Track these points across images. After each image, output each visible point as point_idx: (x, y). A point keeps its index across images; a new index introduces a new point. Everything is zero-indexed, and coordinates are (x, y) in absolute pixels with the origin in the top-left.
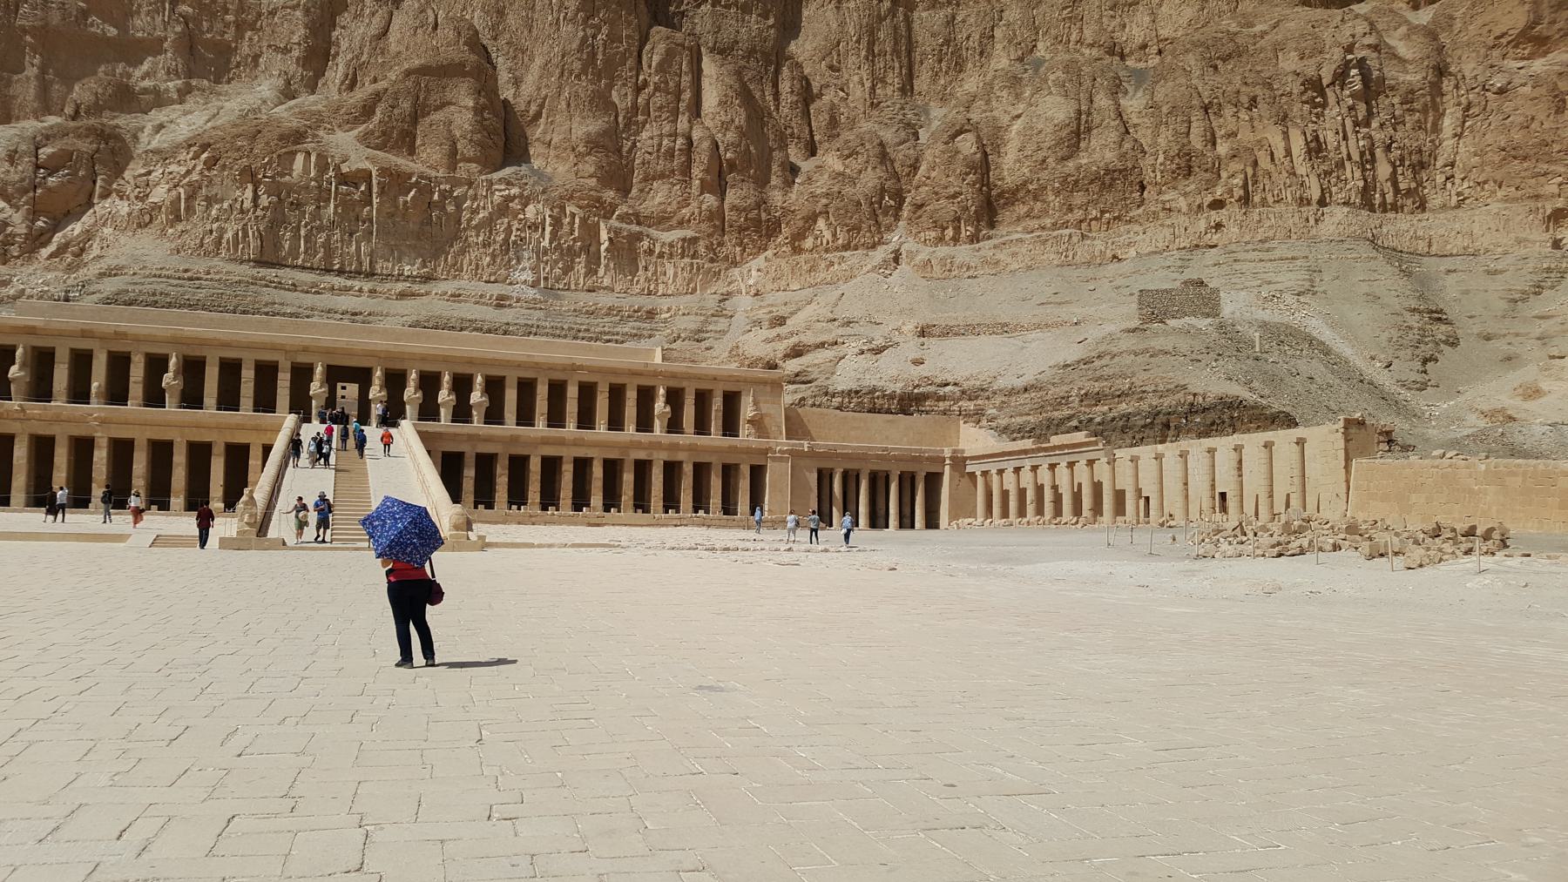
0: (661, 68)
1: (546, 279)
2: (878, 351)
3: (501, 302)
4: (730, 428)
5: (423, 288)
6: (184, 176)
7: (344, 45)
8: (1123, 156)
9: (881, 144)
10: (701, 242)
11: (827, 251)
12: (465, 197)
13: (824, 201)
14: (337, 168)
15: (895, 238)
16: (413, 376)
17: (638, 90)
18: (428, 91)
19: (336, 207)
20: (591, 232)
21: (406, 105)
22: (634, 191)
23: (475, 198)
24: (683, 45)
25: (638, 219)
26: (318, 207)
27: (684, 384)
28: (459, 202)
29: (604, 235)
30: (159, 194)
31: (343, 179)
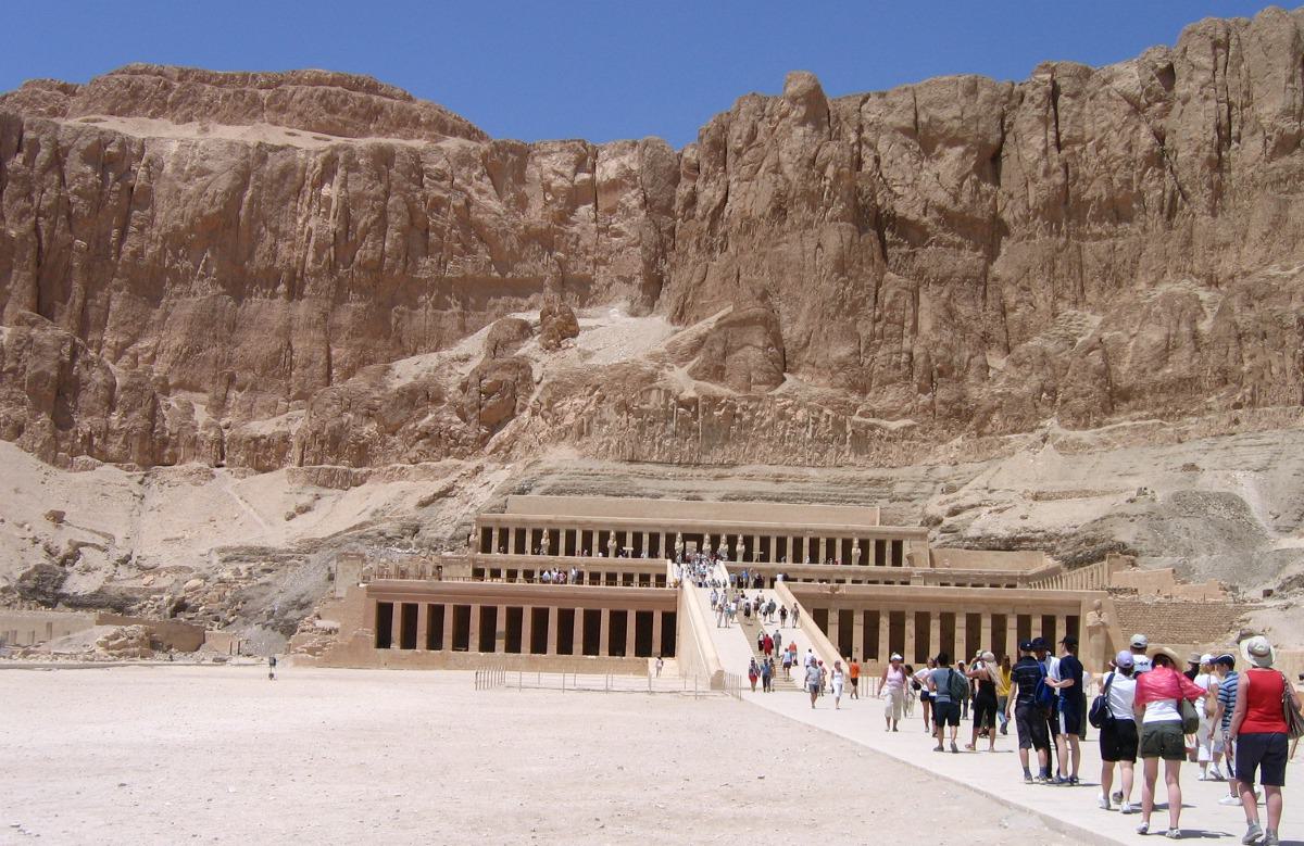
0: (891, 307)
1: (810, 460)
2: (1001, 511)
3: (778, 479)
4: (897, 561)
5: (729, 472)
6: (585, 407)
7: (674, 285)
8: (1191, 369)
9: (1044, 355)
10: (918, 428)
11: (1000, 434)
12: (757, 409)
13: (1000, 399)
14: (677, 398)
15: (1048, 423)
16: (724, 538)
17: (875, 321)
18: (732, 337)
19: (677, 423)
20: (840, 425)
21: (719, 349)
22: (871, 395)
23: (763, 409)
24: (905, 288)
25: (873, 414)
26: (666, 423)
27: (869, 537)
28: (752, 412)
29: (849, 428)
30: (570, 419)
31: (681, 404)
